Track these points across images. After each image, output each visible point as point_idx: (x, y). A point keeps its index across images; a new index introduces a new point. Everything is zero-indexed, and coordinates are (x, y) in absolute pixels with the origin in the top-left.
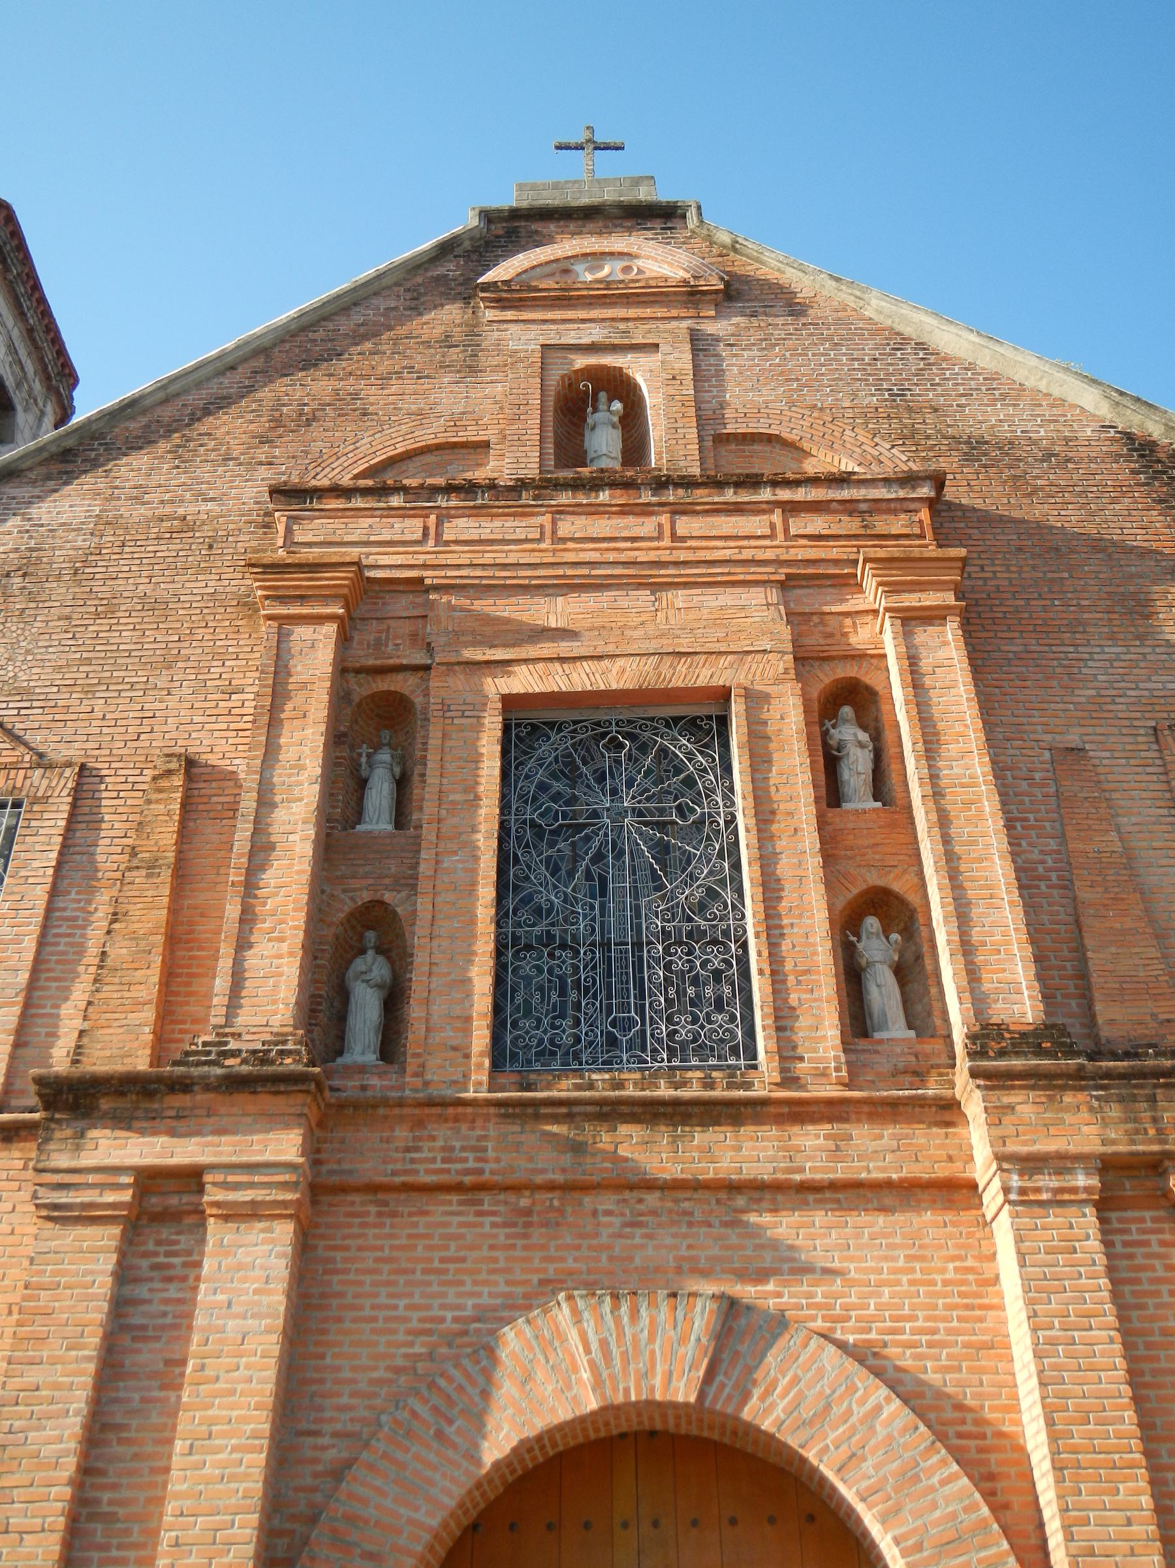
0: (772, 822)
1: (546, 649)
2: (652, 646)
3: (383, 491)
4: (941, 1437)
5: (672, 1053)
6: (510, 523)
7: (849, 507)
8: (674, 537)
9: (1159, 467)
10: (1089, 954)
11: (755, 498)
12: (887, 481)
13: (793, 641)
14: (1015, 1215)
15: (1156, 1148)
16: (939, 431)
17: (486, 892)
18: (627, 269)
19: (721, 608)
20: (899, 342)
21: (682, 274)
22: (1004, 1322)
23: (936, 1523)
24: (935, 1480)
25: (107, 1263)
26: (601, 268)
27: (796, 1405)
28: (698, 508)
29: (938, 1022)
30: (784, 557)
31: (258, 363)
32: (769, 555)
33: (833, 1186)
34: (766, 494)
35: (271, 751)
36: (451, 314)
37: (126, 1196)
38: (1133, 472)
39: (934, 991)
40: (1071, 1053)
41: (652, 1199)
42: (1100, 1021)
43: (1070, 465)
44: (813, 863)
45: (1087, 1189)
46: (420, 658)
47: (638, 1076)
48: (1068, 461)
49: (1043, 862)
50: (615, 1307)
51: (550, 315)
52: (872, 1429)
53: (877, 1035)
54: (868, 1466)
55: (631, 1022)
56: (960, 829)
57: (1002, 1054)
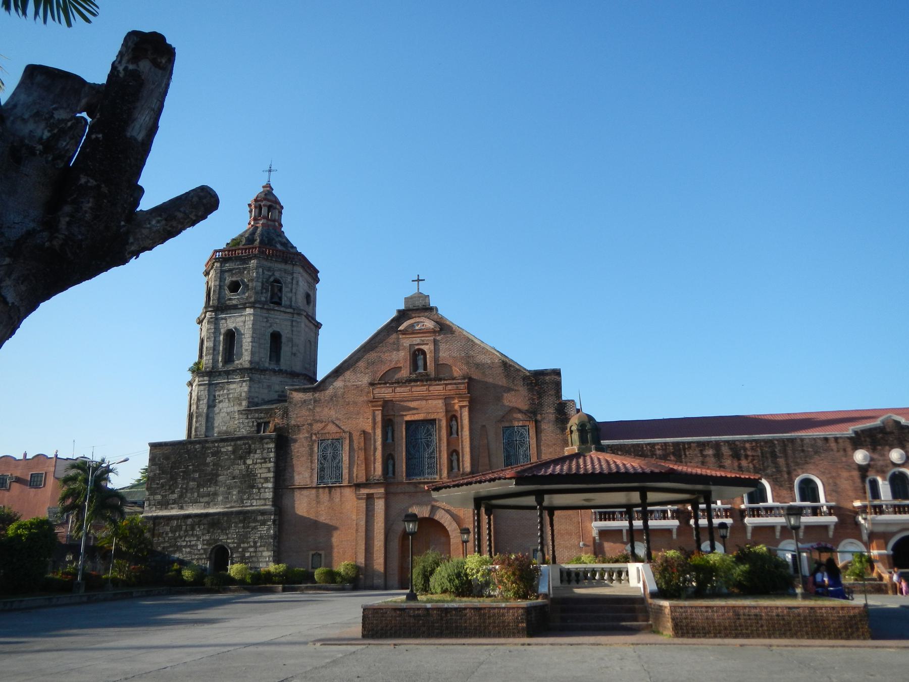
1: (411, 412)
2: (425, 411)
3: (385, 383)
6: (405, 389)
7: (455, 384)
8: (429, 391)
9: (506, 368)
13: (446, 409)
17: (404, 454)
18: (423, 325)
20: (468, 340)
21: (433, 327)
25: (365, 504)
26: (419, 325)
31: (363, 349)
32: (442, 394)
34: (443, 382)
35: (375, 433)
36: (394, 336)
37: (365, 496)
44: (446, 448)
46: (392, 413)
51: (411, 336)
53: (454, 471)
56: (464, 443)
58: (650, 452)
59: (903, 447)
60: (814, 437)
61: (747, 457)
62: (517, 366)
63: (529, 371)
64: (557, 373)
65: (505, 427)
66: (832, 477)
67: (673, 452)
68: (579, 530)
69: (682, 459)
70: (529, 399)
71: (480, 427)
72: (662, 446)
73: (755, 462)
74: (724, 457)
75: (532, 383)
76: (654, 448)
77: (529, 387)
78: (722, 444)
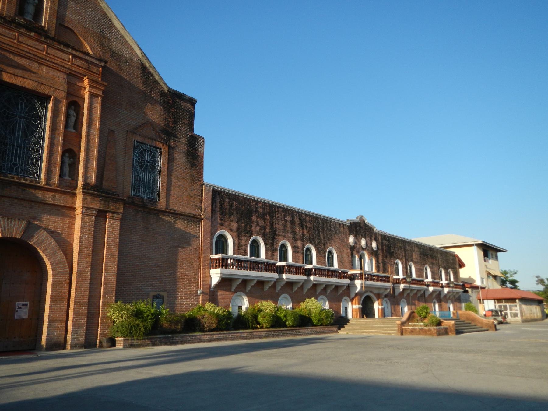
0: (55, 131)
2: (36, 79)
4: (60, 247)
5: (24, 173)
6: (7, 31)
7: (87, 61)
10: (105, 172)
11: (67, 50)
12: (96, 59)
13: (68, 90)
14: (82, 216)
15: (107, 209)
16: (108, 46)
19: (54, 75)
20: (105, 16)
22: (74, 231)
23: (57, 260)
24: (58, 254)
27: (38, 240)
28: (54, 47)
29: (75, 178)
30: (70, 68)
32: (67, 66)
33: (51, 204)
34: (70, 50)
38: (140, 73)
39: (76, 172)
40: (99, 192)
41: (16, 201)
42: (103, 184)
43: (130, 66)
45: (94, 214)
47: (17, 177)
48: (130, 65)
49: (101, 152)
50: (8, 220)
52: (50, 246)
54: (48, 251)
55: (16, 165)
57: (88, 189)
58: (255, 208)
59: (366, 238)
60: (336, 221)
61: (307, 227)
62: (157, 78)
63: (169, 89)
64: (192, 102)
65: (137, 142)
66: (340, 252)
67: (269, 212)
68: (198, 276)
69: (273, 220)
70: (164, 119)
71: (108, 131)
72: (262, 205)
73: (310, 232)
74: (296, 225)
75: (168, 103)
76: (258, 206)
77: (165, 106)
78: (295, 213)
